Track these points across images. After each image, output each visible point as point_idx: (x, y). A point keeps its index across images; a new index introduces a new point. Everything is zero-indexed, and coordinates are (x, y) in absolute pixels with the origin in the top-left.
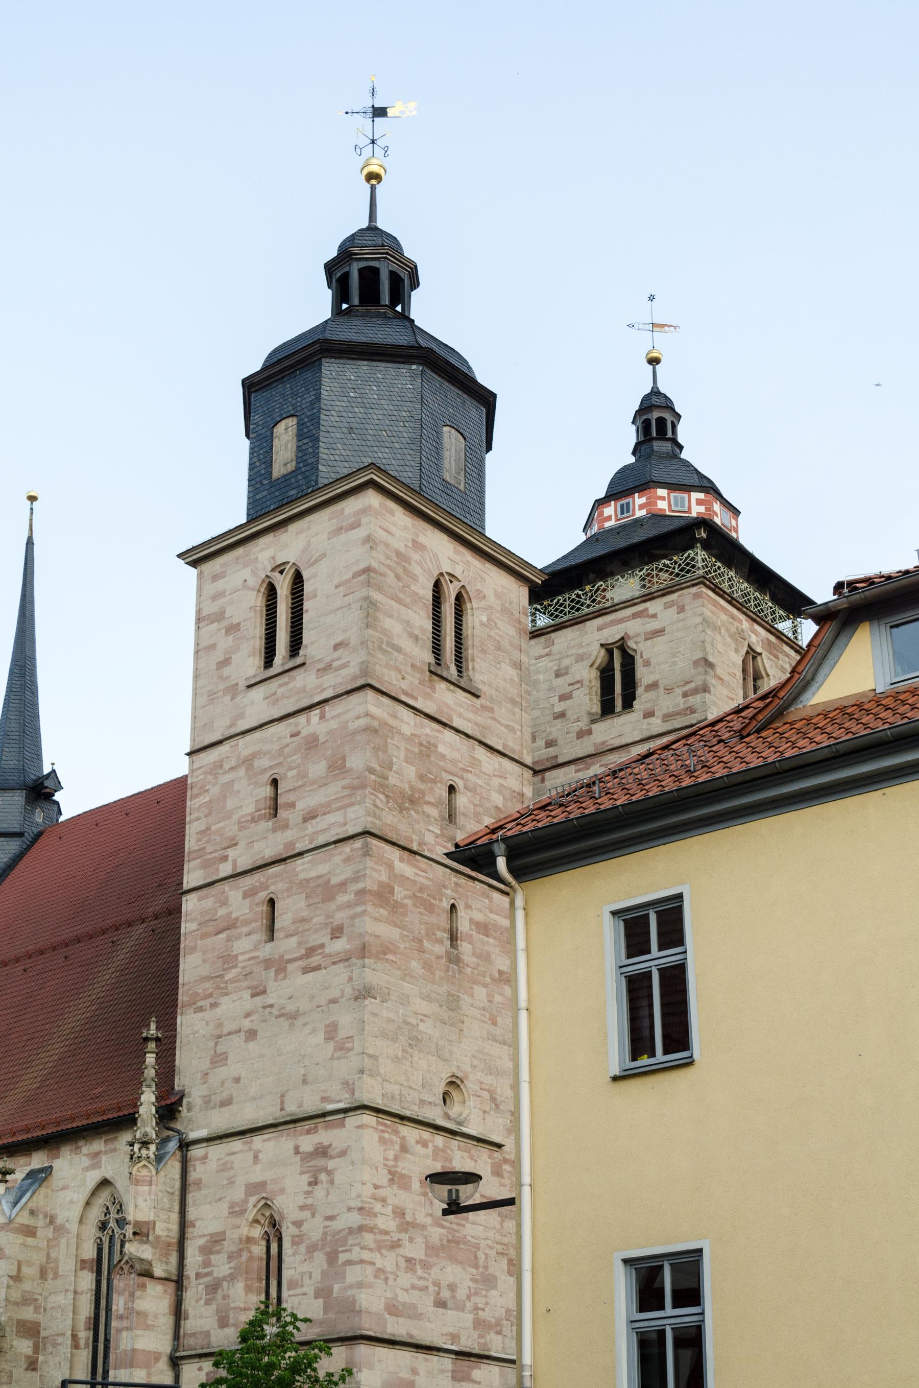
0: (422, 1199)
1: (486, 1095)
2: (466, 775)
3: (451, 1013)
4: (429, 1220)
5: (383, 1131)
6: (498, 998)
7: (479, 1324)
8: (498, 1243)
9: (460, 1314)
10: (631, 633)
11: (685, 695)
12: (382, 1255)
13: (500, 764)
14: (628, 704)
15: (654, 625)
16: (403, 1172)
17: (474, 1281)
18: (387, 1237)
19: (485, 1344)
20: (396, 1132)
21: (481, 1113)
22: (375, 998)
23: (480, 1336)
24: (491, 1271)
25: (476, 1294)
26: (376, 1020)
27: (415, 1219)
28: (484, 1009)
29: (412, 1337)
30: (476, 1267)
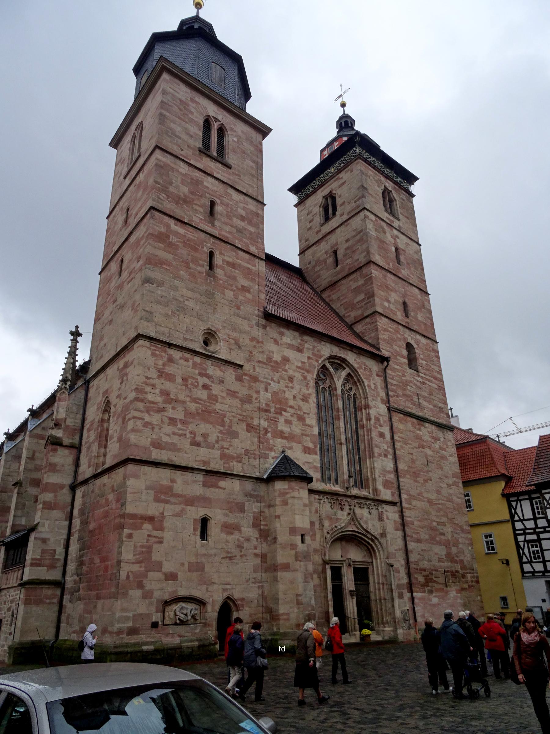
0: (184, 388)
1: (232, 341)
2: (221, 198)
3: (208, 299)
4: (188, 399)
5: (154, 350)
6: (241, 298)
7: (223, 456)
8: (239, 415)
9: (211, 450)
10: (333, 188)
11: (355, 202)
12: (150, 415)
13: (244, 198)
14: (334, 214)
15: (343, 181)
16: (169, 372)
17: (221, 432)
18: (155, 406)
19: (230, 467)
20: (165, 352)
21: (228, 350)
22: (153, 284)
23: (225, 463)
24: (233, 428)
25: (223, 440)
26: (153, 294)
27: (178, 397)
28: (231, 301)
29: (172, 461)
30: (223, 426)
